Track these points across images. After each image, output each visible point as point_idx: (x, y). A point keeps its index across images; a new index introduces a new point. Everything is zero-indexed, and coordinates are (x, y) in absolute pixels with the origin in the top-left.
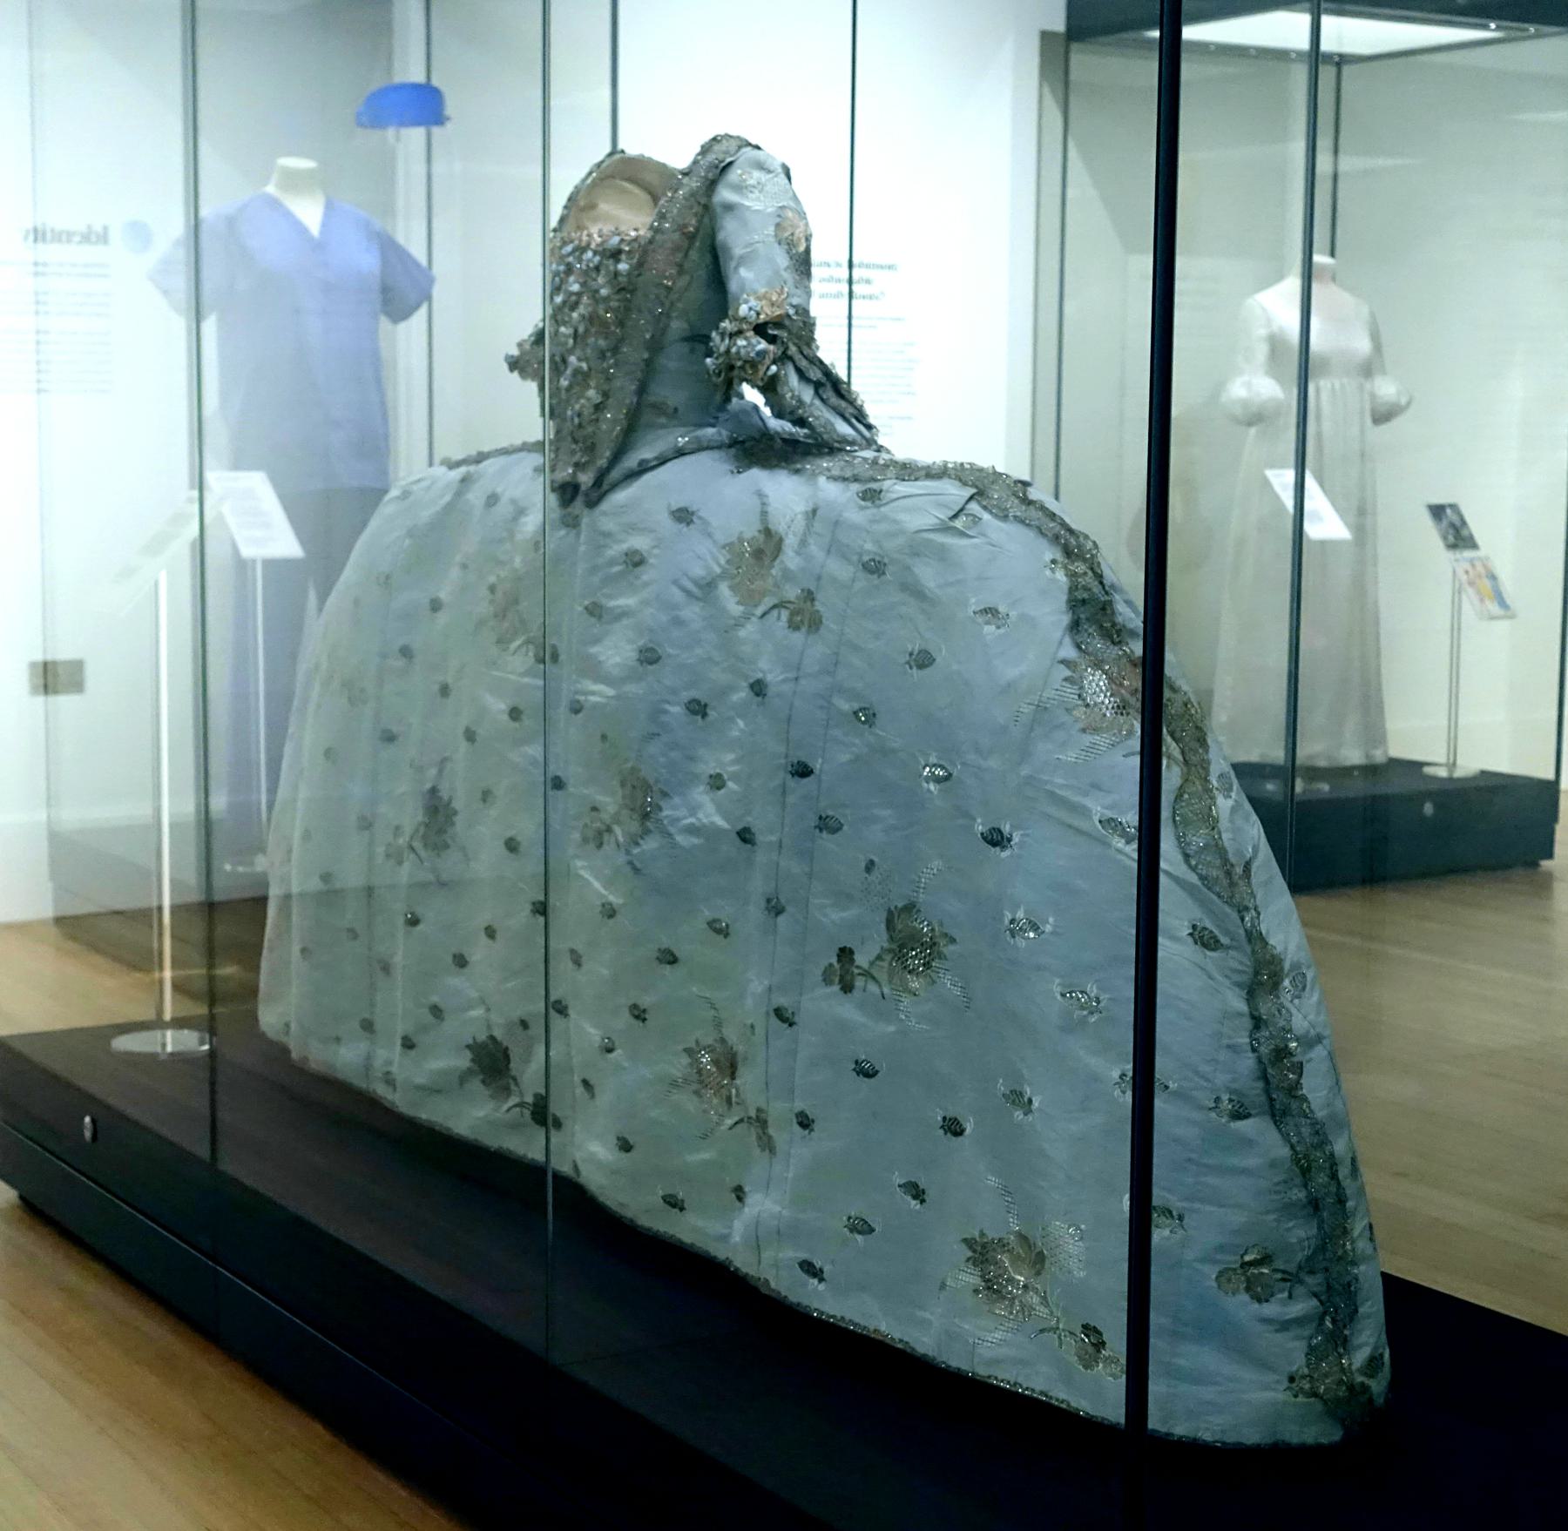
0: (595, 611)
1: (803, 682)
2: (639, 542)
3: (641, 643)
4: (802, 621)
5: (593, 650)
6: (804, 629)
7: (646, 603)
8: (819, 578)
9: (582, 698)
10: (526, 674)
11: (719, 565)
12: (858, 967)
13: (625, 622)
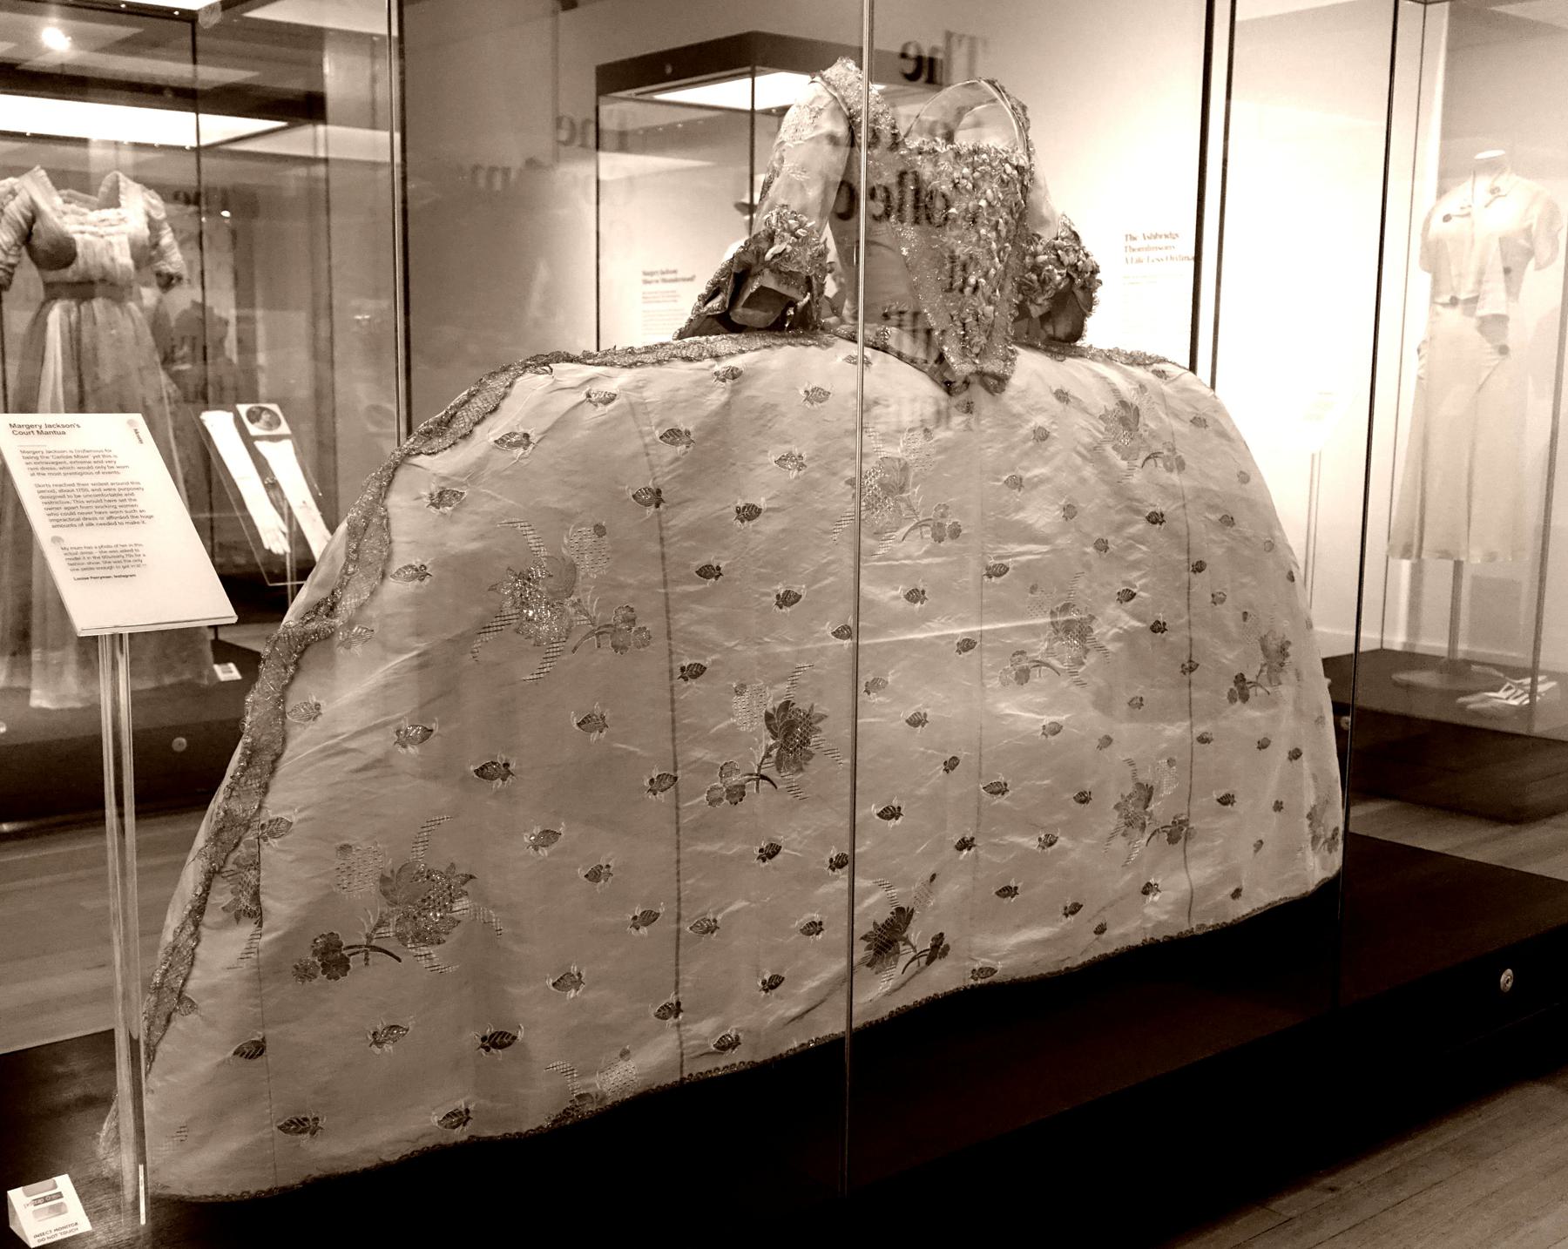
0: (1017, 483)
2: (1040, 420)
3: (1062, 503)
4: (1172, 464)
5: (1020, 516)
6: (1176, 471)
7: (1058, 469)
8: (1173, 434)
9: (1004, 562)
10: (928, 553)
11: (1102, 433)
13: (1042, 488)
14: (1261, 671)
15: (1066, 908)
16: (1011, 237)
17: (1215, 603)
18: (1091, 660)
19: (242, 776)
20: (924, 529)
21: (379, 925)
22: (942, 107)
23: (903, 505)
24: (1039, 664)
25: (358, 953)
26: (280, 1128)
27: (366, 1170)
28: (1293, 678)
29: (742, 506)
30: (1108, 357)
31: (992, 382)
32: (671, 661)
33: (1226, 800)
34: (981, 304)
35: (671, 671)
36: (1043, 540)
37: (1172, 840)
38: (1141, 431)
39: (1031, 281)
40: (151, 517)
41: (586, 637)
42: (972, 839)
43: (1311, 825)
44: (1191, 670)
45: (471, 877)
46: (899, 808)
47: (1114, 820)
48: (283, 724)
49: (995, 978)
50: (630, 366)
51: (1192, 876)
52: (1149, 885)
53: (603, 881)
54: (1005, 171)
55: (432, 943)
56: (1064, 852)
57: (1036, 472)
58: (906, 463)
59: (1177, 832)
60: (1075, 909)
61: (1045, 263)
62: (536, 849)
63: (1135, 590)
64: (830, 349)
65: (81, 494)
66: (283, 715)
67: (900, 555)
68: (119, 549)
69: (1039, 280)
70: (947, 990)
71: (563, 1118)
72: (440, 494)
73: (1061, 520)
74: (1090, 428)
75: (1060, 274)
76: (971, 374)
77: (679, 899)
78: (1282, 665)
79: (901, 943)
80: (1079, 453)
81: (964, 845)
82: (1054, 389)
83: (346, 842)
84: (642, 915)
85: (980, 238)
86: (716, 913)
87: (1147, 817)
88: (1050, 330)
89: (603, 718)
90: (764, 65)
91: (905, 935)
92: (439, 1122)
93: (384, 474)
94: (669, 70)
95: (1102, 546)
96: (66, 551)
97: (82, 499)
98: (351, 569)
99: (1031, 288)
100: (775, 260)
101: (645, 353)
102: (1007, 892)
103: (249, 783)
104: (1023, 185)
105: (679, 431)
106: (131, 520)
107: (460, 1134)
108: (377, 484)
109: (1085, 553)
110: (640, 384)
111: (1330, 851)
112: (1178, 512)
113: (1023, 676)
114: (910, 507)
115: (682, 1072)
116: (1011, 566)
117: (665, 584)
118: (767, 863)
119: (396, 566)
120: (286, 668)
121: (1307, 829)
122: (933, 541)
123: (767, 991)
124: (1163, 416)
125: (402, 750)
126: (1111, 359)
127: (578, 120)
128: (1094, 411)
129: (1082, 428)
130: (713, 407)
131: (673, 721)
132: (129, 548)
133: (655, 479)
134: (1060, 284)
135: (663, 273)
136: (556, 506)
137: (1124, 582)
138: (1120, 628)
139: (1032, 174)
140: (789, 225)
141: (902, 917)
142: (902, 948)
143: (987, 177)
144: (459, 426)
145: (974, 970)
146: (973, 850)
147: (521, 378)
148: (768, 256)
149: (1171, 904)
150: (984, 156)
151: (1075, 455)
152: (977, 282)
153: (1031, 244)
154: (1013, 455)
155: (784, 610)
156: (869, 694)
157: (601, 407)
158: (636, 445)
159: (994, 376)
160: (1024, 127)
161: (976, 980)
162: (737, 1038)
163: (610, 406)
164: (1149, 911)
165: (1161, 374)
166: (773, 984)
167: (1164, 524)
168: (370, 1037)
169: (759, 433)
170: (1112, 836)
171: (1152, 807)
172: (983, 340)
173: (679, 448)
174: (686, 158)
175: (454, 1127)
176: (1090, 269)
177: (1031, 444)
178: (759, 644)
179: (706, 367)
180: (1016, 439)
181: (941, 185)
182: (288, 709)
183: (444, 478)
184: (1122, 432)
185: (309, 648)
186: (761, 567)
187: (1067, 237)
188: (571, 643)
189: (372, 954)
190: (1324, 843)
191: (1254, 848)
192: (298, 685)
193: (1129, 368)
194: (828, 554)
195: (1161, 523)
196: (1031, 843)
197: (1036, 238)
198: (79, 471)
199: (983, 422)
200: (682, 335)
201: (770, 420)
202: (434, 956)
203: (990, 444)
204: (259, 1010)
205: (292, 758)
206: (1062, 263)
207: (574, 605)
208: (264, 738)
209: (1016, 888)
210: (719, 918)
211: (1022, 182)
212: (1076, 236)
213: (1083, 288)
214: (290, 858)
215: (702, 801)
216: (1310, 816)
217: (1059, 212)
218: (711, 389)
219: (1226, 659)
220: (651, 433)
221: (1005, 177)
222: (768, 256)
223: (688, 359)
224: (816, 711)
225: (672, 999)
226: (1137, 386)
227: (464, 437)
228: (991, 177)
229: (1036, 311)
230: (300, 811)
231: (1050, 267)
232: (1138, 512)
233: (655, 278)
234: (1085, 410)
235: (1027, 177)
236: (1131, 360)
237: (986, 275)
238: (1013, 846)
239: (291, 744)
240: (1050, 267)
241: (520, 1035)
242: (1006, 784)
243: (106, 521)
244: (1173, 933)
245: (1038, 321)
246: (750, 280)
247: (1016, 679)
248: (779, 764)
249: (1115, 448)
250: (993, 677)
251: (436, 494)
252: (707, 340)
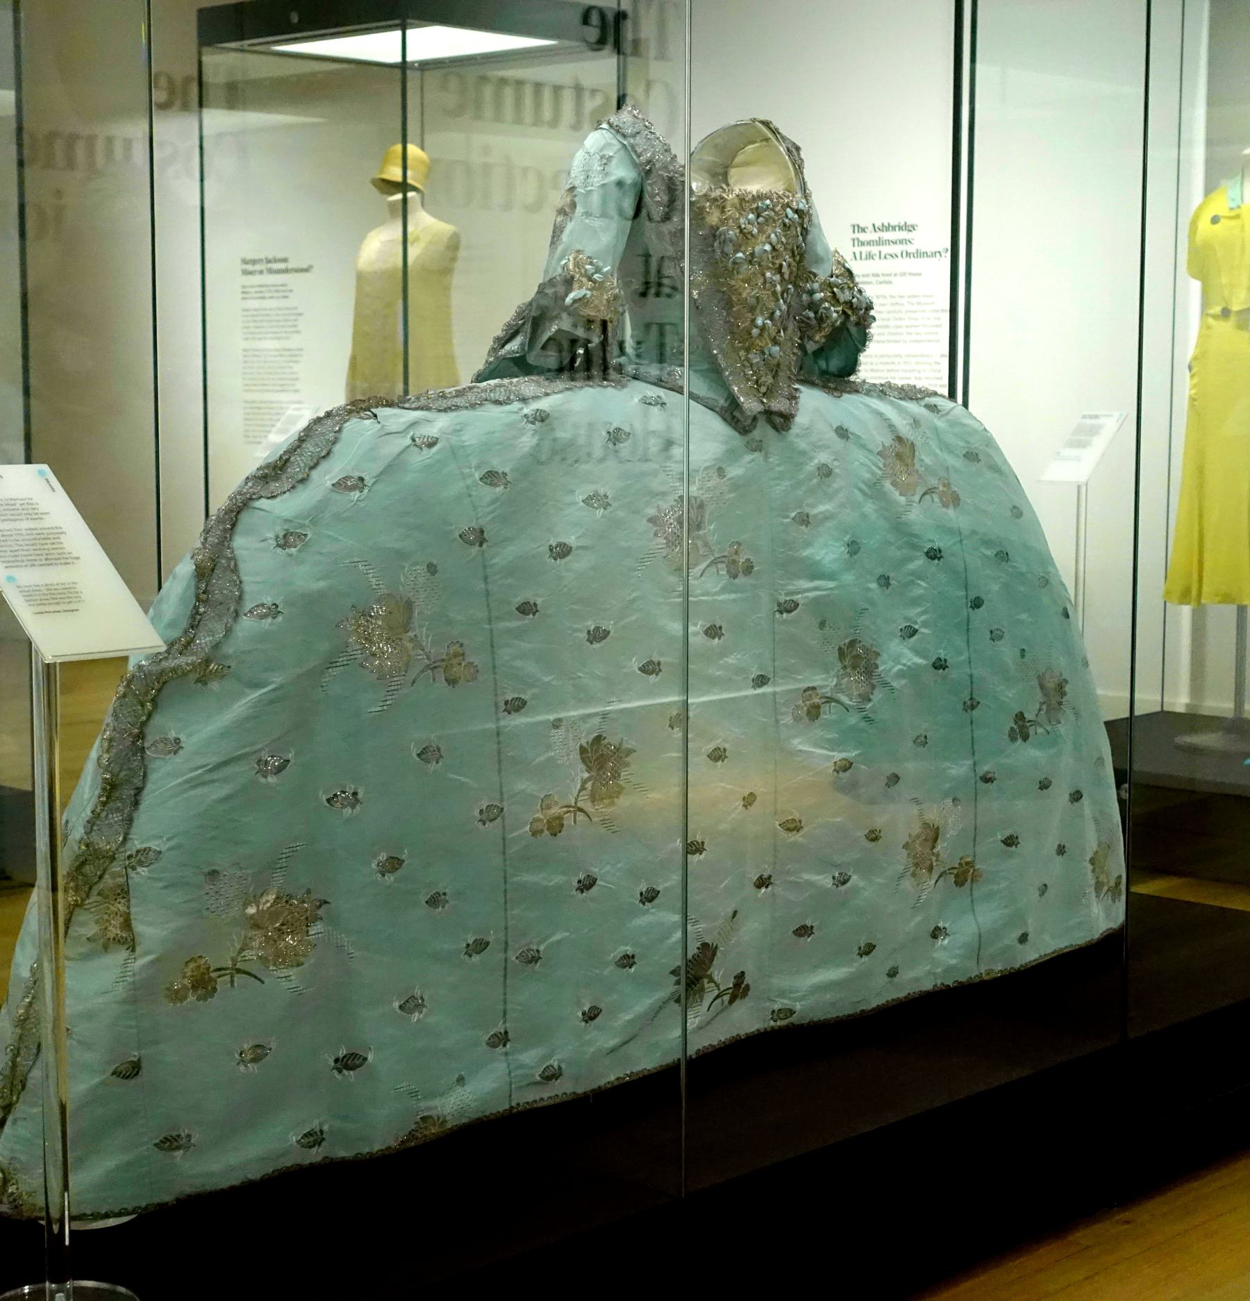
0: (804, 520)
1: (965, 542)
2: (823, 457)
3: (847, 538)
5: (806, 553)
6: (951, 506)
7: (842, 505)
8: (948, 468)
9: (795, 598)
10: (724, 590)
11: (880, 469)
12: (1029, 721)
13: (829, 524)
14: (1040, 710)
15: (860, 948)
16: (793, 279)
17: (993, 640)
18: (877, 696)
19: (103, 810)
20: (720, 566)
21: (242, 950)
22: (716, 146)
23: (699, 543)
24: (830, 700)
25: (224, 975)
26: (156, 1145)
27: (233, 1189)
28: (1072, 717)
29: (554, 545)
30: (883, 391)
31: (778, 420)
32: (496, 695)
33: (1010, 841)
34: (767, 344)
35: (496, 704)
36: (831, 576)
37: (960, 881)
38: (917, 467)
39: (809, 318)
40: (78, 558)
41: (422, 671)
42: (770, 877)
43: (1093, 871)
44: (973, 707)
45: (326, 902)
46: (703, 843)
47: (901, 860)
48: (143, 758)
49: (794, 1019)
50: (445, 410)
51: (980, 919)
52: (937, 928)
53: (440, 908)
54: (787, 217)
55: (292, 966)
56: (856, 890)
57: (822, 508)
58: (702, 501)
59: (964, 875)
60: (868, 950)
61: (823, 300)
62: (383, 875)
63: (917, 627)
64: (625, 390)
65: (19, 538)
66: (143, 749)
67: (698, 591)
68: (60, 587)
69: (816, 318)
70: (748, 1032)
71: (408, 1140)
72: (285, 536)
73: (847, 556)
74: (869, 463)
75: (837, 312)
76: (760, 413)
77: (506, 928)
78: (1060, 703)
79: (706, 981)
80: (861, 490)
81: (762, 882)
82: (835, 427)
83: (213, 868)
84: (474, 943)
85: (765, 282)
86: (539, 943)
87: (934, 858)
88: (823, 364)
89: (439, 749)
90: (419, 18)
91: (709, 973)
92: (298, 1142)
93: (227, 517)
94: (295, 18)
95: (885, 581)
96: (20, 589)
97: (20, 543)
98: (202, 610)
99: (808, 325)
100: (576, 305)
101: (456, 396)
102: (804, 931)
103: (110, 816)
104: (803, 228)
105: (497, 473)
106: (63, 561)
107: (315, 1155)
108: (221, 527)
109: (868, 590)
110: (458, 427)
111: (1114, 901)
112: (955, 548)
113: (814, 713)
114: (706, 545)
115: (510, 1101)
116: (801, 602)
117: (490, 620)
118: (584, 894)
119: (248, 605)
120: (143, 705)
121: (1090, 875)
122: (727, 577)
123: (586, 1022)
124: (938, 451)
125: (263, 780)
126: (886, 394)
127: (178, 78)
128: (871, 447)
129: (862, 465)
130: (526, 449)
131: (499, 753)
132: (67, 586)
133: (477, 519)
134: (836, 321)
135: (269, 261)
136: (398, 545)
137: (907, 619)
138: (904, 665)
139: (811, 215)
140: (586, 270)
141: (708, 952)
142: (706, 985)
143: (771, 221)
144: (295, 469)
145: (774, 1011)
146: (770, 888)
147: (348, 424)
148: (568, 300)
149: (959, 948)
150: (768, 202)
151: (856, 491)
152: (764, 324)
153: (807, 282)
154: (800, 493)
155: (594, 646)
156: (673, 728)
157: (425, 450)
158: (457, 487)
159: (781, 415)
160: (799, 168)
161: (775, 1021)
162: (560, 1068)
163: (435, 449)
164: (939, 955)
165: (933, 408)
166: (591, 1015)
167: (942, 560)
168: (237, 1056)
170: (901, 877)
171: (938, 848)
172: (770, 380)
173: (498, 489)
174: (298, 114)
175: (311, 1147)
176: (864, 305)
177: (815, 481)
178: (573, 679)
179: (515, 410)
180: (802, 476)
181: (728, 230)
182: (146, 745)
183: (287, 521)
184: (899, 466)
185: (166, 686)
186: (573, 604)
187: (841, 275)
188: (412, 674)
189: (237, 977)
190: (1108, 890)
191: (1038, 893)
192: (158, 720)
193: (903, 403)
194: (634, 591)
195: (939, 559)
196: (826, 881)
197: (812, 276)
198: (12, 518)
199: (771, 460)
200: (480, 378)
202: (293, 978)
203: (778, 482)
204: (135, 1031)
205: (155, 791)
206: (838, 301)
207: (411, 640)
208: (122, 774)
209: (812, 927)
210: (542, 948)
211: (802, 225)
212: (850, 273)
213: (857, 324)
214: (161, 884)
215: (526, 832)
216: (1092, 861)
217: (832, 249)
218: (522, 432)
219: (1007, 697)
220: (471, 475)
221: (787, 221)
222: (568, 300)
223: (498, 402)
224: (625, 746)
225: (500, 1028)
226: (912, 421)
227: (302, 481)
228: (774, 221)
229: (811, 347)
230: (169, 840)
231: (827, 305)
232: (914, 547)
233: (258, 267)
234: (863, 447)
235: (806, 220)
236: (903, 395)
237: (771, 317)
238: (809, 884)
239: (152, 777)
240: (827, 305)
241: (370, 1057)
242: (800, 821)
243: (44, 562)
244: (963, 979)
245: (812, 357)
246: (547, 324)
247: (807, 715)
248: (593, 799)
249: (894, 484)
250: (786, 713)
251: (281, 535)
252: (511, 383)
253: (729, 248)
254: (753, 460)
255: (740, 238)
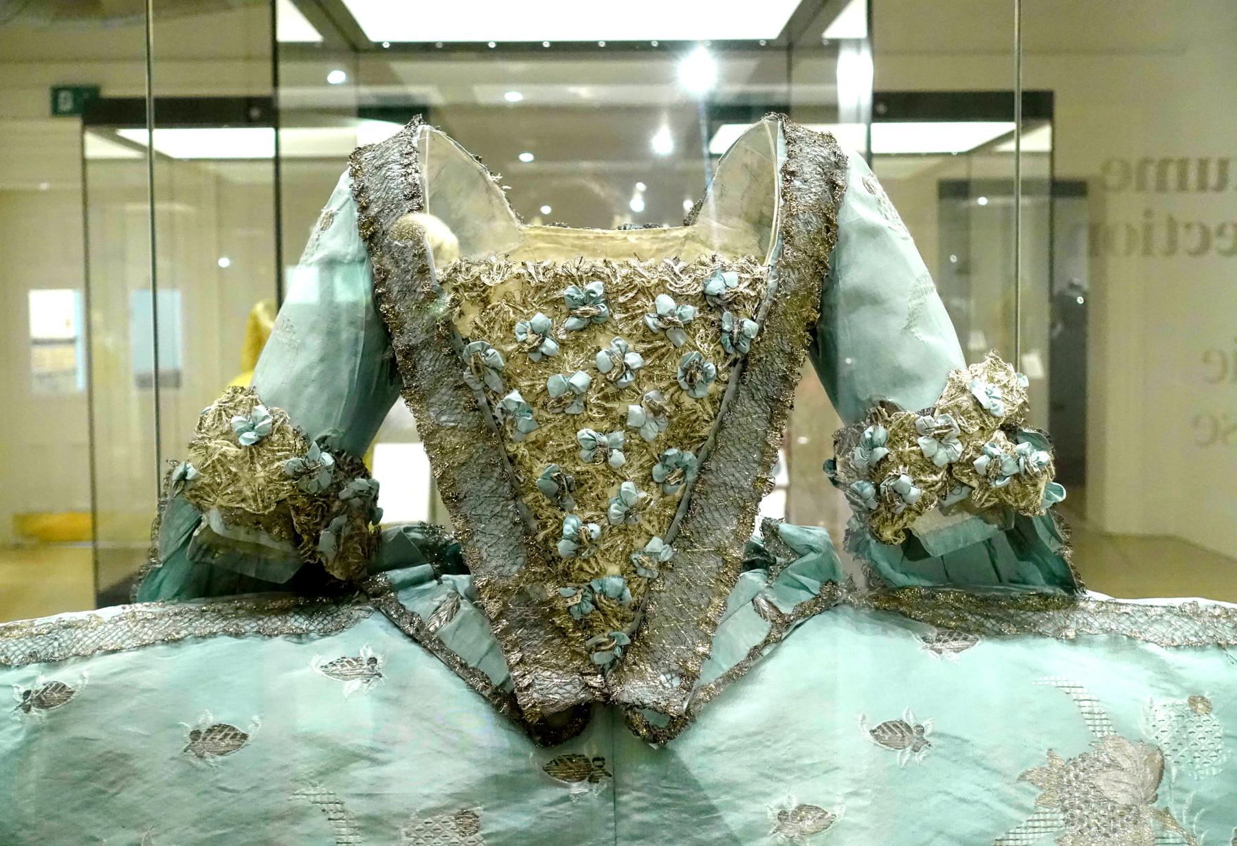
169: (88, 805)
180: (717, 834)
199: (624, 798)
201: (113, 783)
253: (496, 382)
254: (566, 799)
255: (519, 362)
